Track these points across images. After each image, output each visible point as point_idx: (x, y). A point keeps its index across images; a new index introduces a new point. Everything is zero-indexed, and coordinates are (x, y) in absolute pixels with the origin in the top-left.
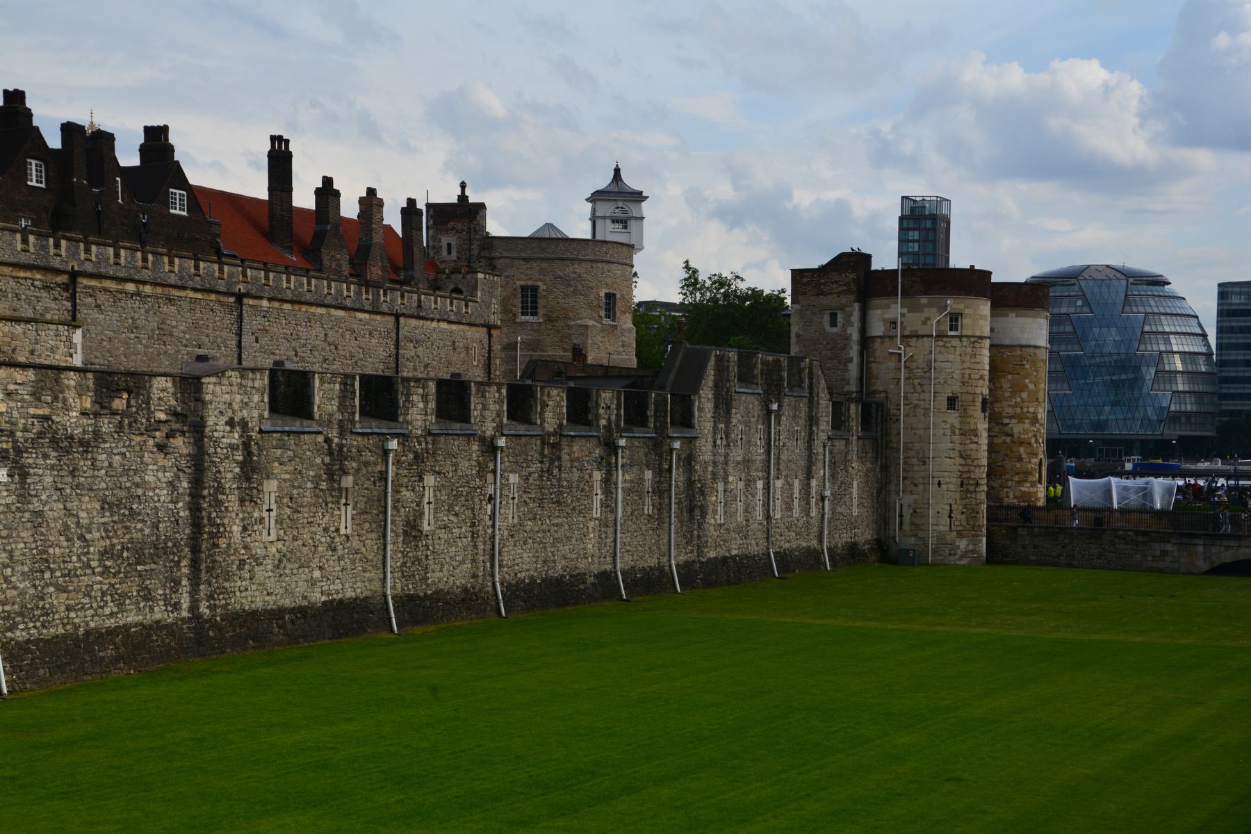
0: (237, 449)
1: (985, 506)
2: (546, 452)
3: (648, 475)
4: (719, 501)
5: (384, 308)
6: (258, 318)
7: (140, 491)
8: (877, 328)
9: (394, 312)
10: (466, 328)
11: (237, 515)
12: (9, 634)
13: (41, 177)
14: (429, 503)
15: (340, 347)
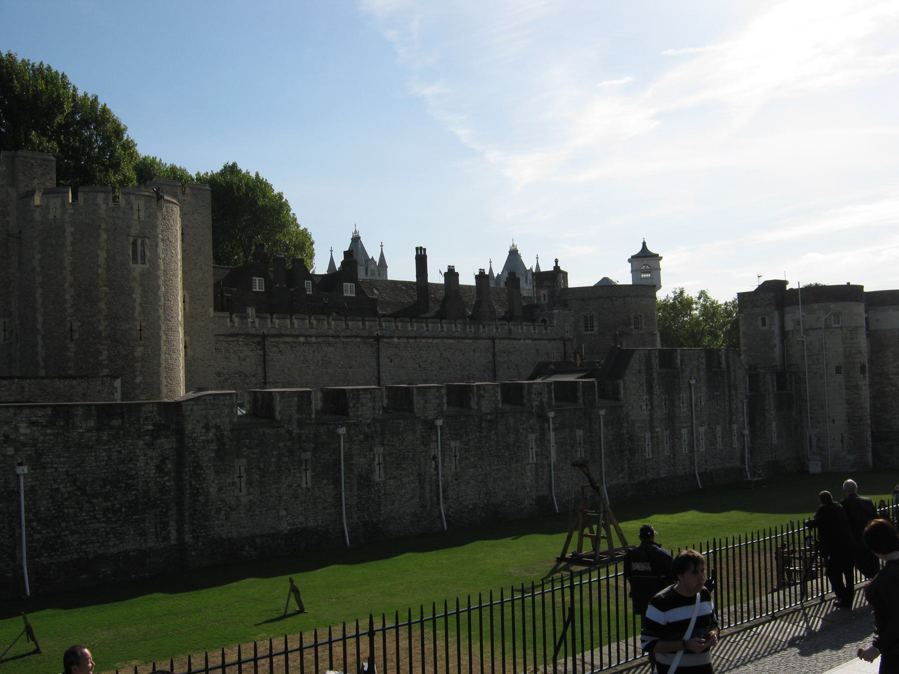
0: (212, 441)
1: (870, 433)
2: (484, 425)
3: (580, 433)
4: (647, 444)
5: (484, 335)
6: (392, 349)
7: (133, 472)
8: (789, 326)
9: (491, 337)
10: (546, 342)
11: (213, 481)
12: (37, 559)
13: (262, 286)
14: (379, 464)
15: (451, 360)
